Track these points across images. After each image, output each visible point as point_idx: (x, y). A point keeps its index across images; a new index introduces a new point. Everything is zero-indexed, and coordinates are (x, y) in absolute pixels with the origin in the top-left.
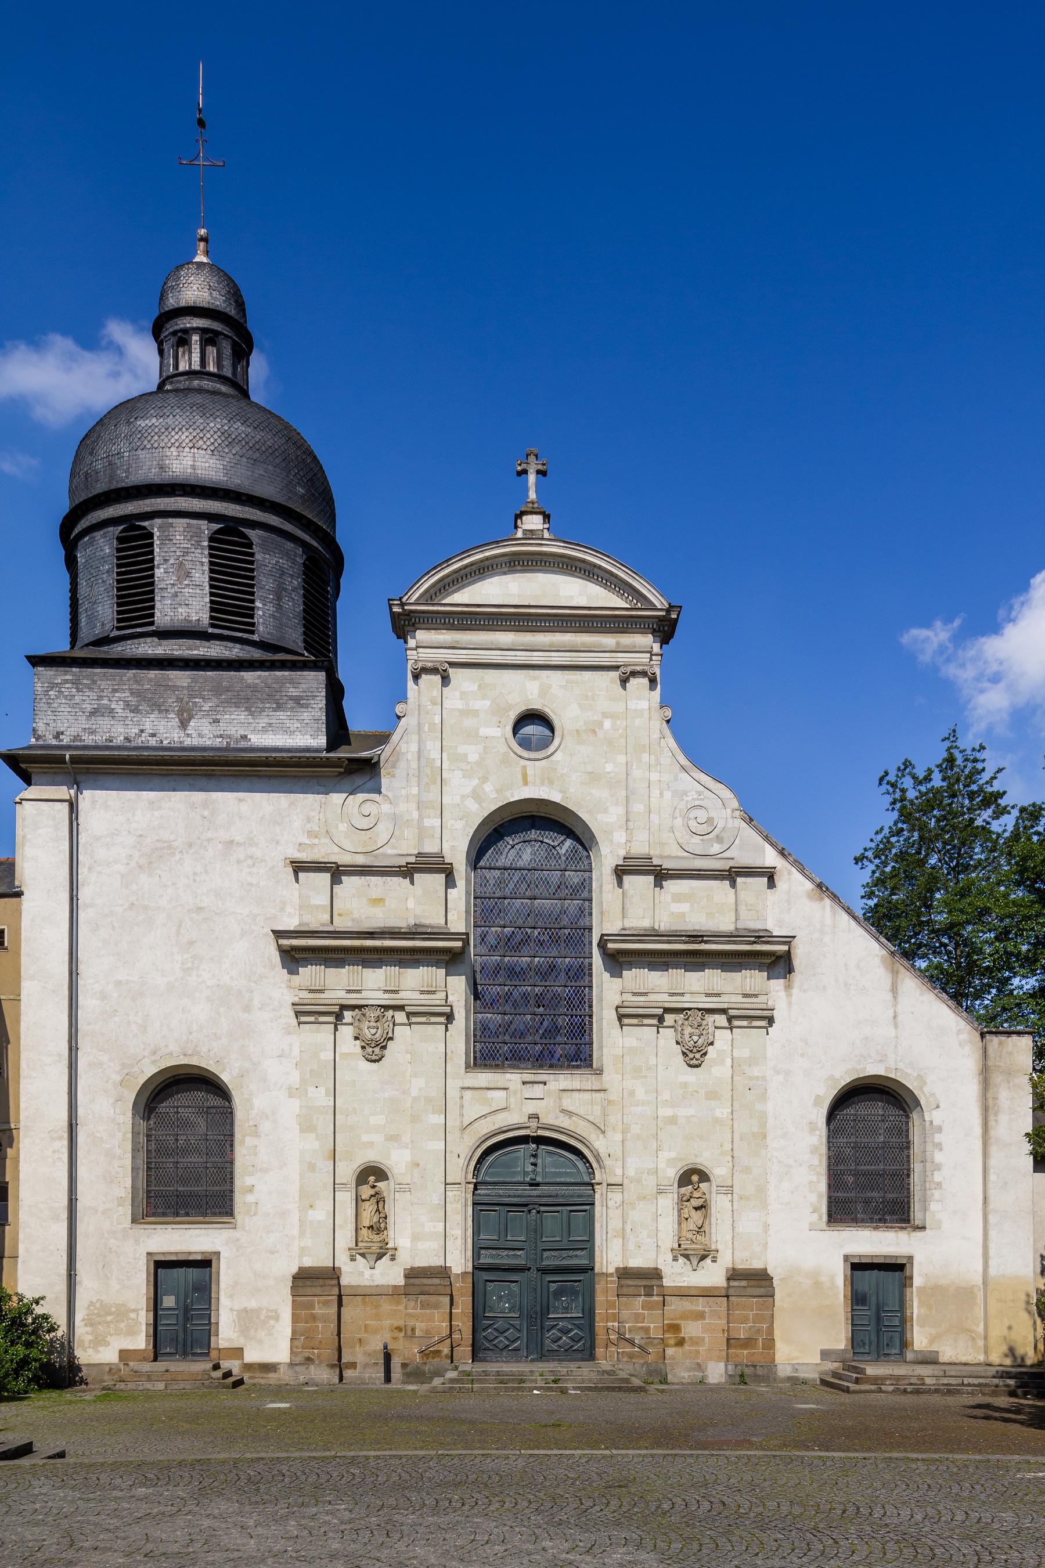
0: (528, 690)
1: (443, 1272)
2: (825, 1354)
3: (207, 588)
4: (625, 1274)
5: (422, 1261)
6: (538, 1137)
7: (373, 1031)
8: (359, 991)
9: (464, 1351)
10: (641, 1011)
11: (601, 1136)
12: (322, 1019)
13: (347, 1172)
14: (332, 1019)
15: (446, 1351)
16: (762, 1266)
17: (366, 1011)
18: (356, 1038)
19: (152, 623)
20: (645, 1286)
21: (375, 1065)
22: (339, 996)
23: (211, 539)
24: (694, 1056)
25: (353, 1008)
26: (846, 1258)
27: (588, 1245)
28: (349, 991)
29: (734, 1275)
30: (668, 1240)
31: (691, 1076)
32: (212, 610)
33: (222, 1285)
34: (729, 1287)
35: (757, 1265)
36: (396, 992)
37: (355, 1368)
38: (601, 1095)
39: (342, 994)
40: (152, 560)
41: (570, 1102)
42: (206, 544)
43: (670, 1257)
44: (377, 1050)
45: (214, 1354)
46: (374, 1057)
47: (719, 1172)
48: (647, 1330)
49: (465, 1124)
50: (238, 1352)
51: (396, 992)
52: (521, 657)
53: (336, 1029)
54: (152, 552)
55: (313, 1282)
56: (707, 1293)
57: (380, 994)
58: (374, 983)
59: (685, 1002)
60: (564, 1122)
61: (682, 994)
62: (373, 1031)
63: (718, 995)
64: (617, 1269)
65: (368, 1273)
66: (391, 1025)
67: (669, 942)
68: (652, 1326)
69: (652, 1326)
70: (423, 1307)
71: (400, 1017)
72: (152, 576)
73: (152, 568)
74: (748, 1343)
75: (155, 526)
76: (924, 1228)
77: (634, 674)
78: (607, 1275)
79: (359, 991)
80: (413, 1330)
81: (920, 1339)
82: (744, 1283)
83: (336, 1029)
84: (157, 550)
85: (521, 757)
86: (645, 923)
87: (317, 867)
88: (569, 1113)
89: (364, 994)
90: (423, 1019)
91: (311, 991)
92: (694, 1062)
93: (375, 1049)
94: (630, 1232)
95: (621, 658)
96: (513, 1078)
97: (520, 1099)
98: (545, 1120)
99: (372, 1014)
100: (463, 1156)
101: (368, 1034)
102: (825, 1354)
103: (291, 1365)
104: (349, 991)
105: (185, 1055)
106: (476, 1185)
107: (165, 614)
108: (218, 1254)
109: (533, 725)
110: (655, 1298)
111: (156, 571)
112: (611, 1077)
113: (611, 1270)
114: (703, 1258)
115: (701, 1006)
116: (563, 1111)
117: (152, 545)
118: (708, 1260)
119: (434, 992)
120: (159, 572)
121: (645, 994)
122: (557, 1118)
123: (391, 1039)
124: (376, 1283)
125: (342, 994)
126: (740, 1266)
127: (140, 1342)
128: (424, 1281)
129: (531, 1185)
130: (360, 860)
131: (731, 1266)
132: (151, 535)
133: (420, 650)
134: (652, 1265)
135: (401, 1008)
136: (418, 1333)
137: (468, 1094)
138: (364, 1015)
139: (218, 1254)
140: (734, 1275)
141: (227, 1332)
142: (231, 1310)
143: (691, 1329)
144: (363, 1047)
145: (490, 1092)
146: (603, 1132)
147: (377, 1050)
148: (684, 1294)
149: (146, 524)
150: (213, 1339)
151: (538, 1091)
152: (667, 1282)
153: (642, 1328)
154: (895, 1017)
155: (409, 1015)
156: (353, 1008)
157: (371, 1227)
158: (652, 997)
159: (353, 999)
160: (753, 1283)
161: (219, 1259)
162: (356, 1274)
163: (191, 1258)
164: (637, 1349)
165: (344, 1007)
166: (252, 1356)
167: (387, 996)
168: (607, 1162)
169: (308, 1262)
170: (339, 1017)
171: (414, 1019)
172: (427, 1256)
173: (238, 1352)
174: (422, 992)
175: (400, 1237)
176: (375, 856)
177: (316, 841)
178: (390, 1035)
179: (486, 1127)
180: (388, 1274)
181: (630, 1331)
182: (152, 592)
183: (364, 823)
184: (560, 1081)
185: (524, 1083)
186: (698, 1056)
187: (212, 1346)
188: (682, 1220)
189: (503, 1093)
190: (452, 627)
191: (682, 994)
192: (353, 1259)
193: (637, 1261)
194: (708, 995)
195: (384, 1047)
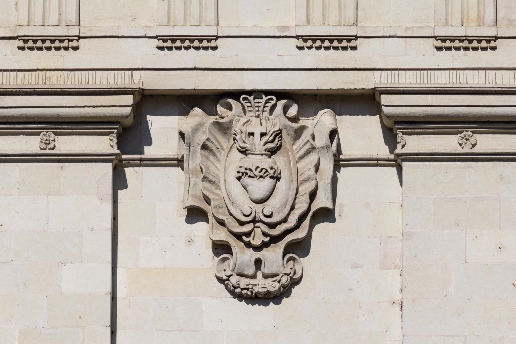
7: (260, 187)
8: (205, 43)
12: (68, 144)
14: (104, 144)
18: (195, 214)
25: (182, 102)
28: (170, 43)
39: (146, 53)
44: (273, 256)
46: (261, 285)
53: (119, 182)
57: (287, 53)
62: (260, 187)
66: (327, 165)
71: (362, 134)
79: (205, 43)
83: (119, 182)
89: (227, 53)
90: (448, 143)
99: (254, 123)
101: (238, 199)
104: (170, 43)
123: (326, 215)
125: (146, 53)
135: (365, 102)
138: (224, 128)
144: (221, 248)
147: (273, 256)
155: (394, 128)
156: (182, 102)
165: (149, 102)
170: (131, 135)
171: (413, 143)
178: (323, 201)
195: (300, 248)
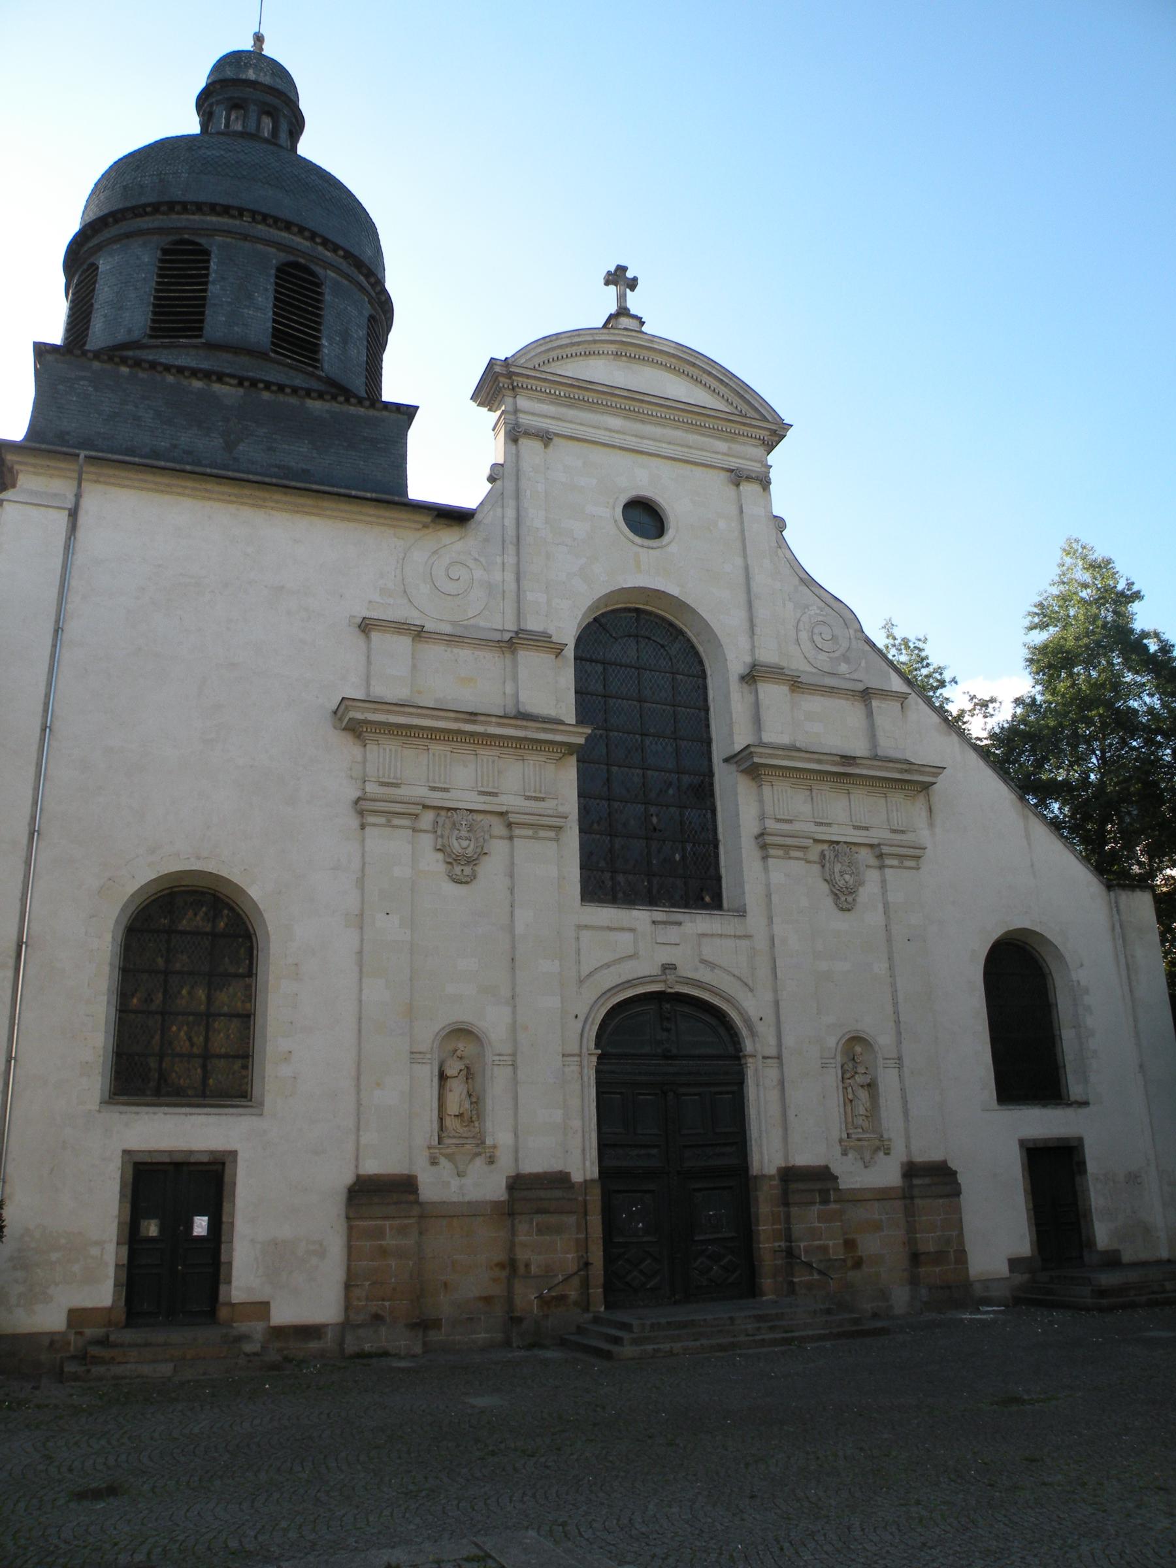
0: (643, 479)
1: (560, 1180)
2: (1014, 1263)
3: (271, 314)
4: (789, 1175)
5: (533, 1165)
6: (678, 994)
9: (597, 1292)
10: (789, 841)
11: (750, 994)
13: (427, 1033)
15: (573, 1294)
16: (942, 1158)
17: (456, 817)
19: (200, 336)
20: (820, 1191)
21: (461, 890)
22: (421, 792)
23: (278, 270)
24: (844, 898)
26: (1022, 1143)
27: (737, 1137)
29: (911, 1171)
30: (836, 1130)
31: (840, 923)
32: (274, 336)
33: (240, 1202)
34: (911, 1186)
35: (935, 1156)
36: (495, 794)
37: (439, 1328)
38: (744, 943)
40: (207, 276)
41: (709, 950)
42: (273, 272)
43: (838, 1150)
45: (223, 1313)
47: (884, 1040)
48: (824, 1249)
49: (584, 973)
50: (263, 1308)
51: (495, 794)
52: (631, 442)
54: (207, 268)
55: (377, 1197)
56: (882, 1195)
57: (474, 796)
58: (464, 778)
59: (834, 833)
60: (704, 975)
61: (829, 825)
62: (465, 843)
63: (867, 828)
64: (780, 1170)
65: (455, 1183)
67: (819, 762)
68: (831, 1243)
69: (831, 1243)
70: (540, 1232)
72: (205, 291)
73: (206, 283)
74: (939, 1257)
75: (214, 245)
76: (1086, 1104)
77: (749, 478)
78: (771, 1177)
80: (527, 1266)
81: (1103, 1234)
82: (927, 1181)
84: (213, 266)
85: (633, 542)
86: (785, 740)
87: (400, 627)
88: (712, 966)
91: (383, 784)
92: (845, 906)
93: (463, 866)
94: (791, 1122)
95: (734, 463)
96: (640, 917)
97: (642, 946)
98: (686, 971)
100: (582, 1018)
102: (1014, 1263)
103: (346, 1326)
104: (433, 789)
105: (198, 858)
106: (600, 1057)
107: (216, 324)
108: (234, 1153)
109: (645, 517)
110: (833, 1206)
111: (210, 287)
112: (755, 919)
113: (772, 1171)
114: (878, 1149)
115: (849, 840)
116: (703, 961)
117: (208, 261)
118: (881, 1154)
119: (543, 799)
120: (214, 289)
121: (790, 821)
122: (696, 969)
124: (467, 1199)
126: (919, 1158)
127: (102, 1293)
128: (531, 1194)
129: (666, 1057)
130: (447, 628)
131: (905, 1159)
132: (207, 253)
133: (521, 415)
134: (822, 1162)
136: (534, 1269)
137: (585, 935)
139: (234, 1153)
140: (911, 1171)
141: (245, 1278)
142: (253, 1241)
143: (870, 1245)
145: (612, 933)
146: (751, 990)
147: (468, 870)
148: (858, 1198)
149: (202, 241)
150: (223, 1288)
151: (672, 934)
152: (844, 1184)
153: (819, 1247)
154: (1032, 865)
157: (460, 1116)
158: (797, 827)
159: (437, 798)
160: (932, 1181)
161: (235, 1161)
162: (438, 1184)
163: (192, 1160)
164: (816, 1277)
166: (283, 1314)
167: (483, 798)
168: (761, 1028)
169: (372, 1167)
172: (539, 1159)
173: (263, 1308)
174: (528, 798)
175: (499, 1134)
176: (466, 627)
177: (391, 601)
179: (609, 979)
180: (488, 1185)
181: (806, 1252)
182: (203, 306)
183: (451, 587)
184: (698, 923)
185: (654, 922)
186: (850, 899)
187: (222, 1298)
188: (849, 1102)
189: (627, 937)
190: (555, 399)
191: (829, 825)
192: (434, 1162)
193: (804, 1158)
194: (855, 827)
